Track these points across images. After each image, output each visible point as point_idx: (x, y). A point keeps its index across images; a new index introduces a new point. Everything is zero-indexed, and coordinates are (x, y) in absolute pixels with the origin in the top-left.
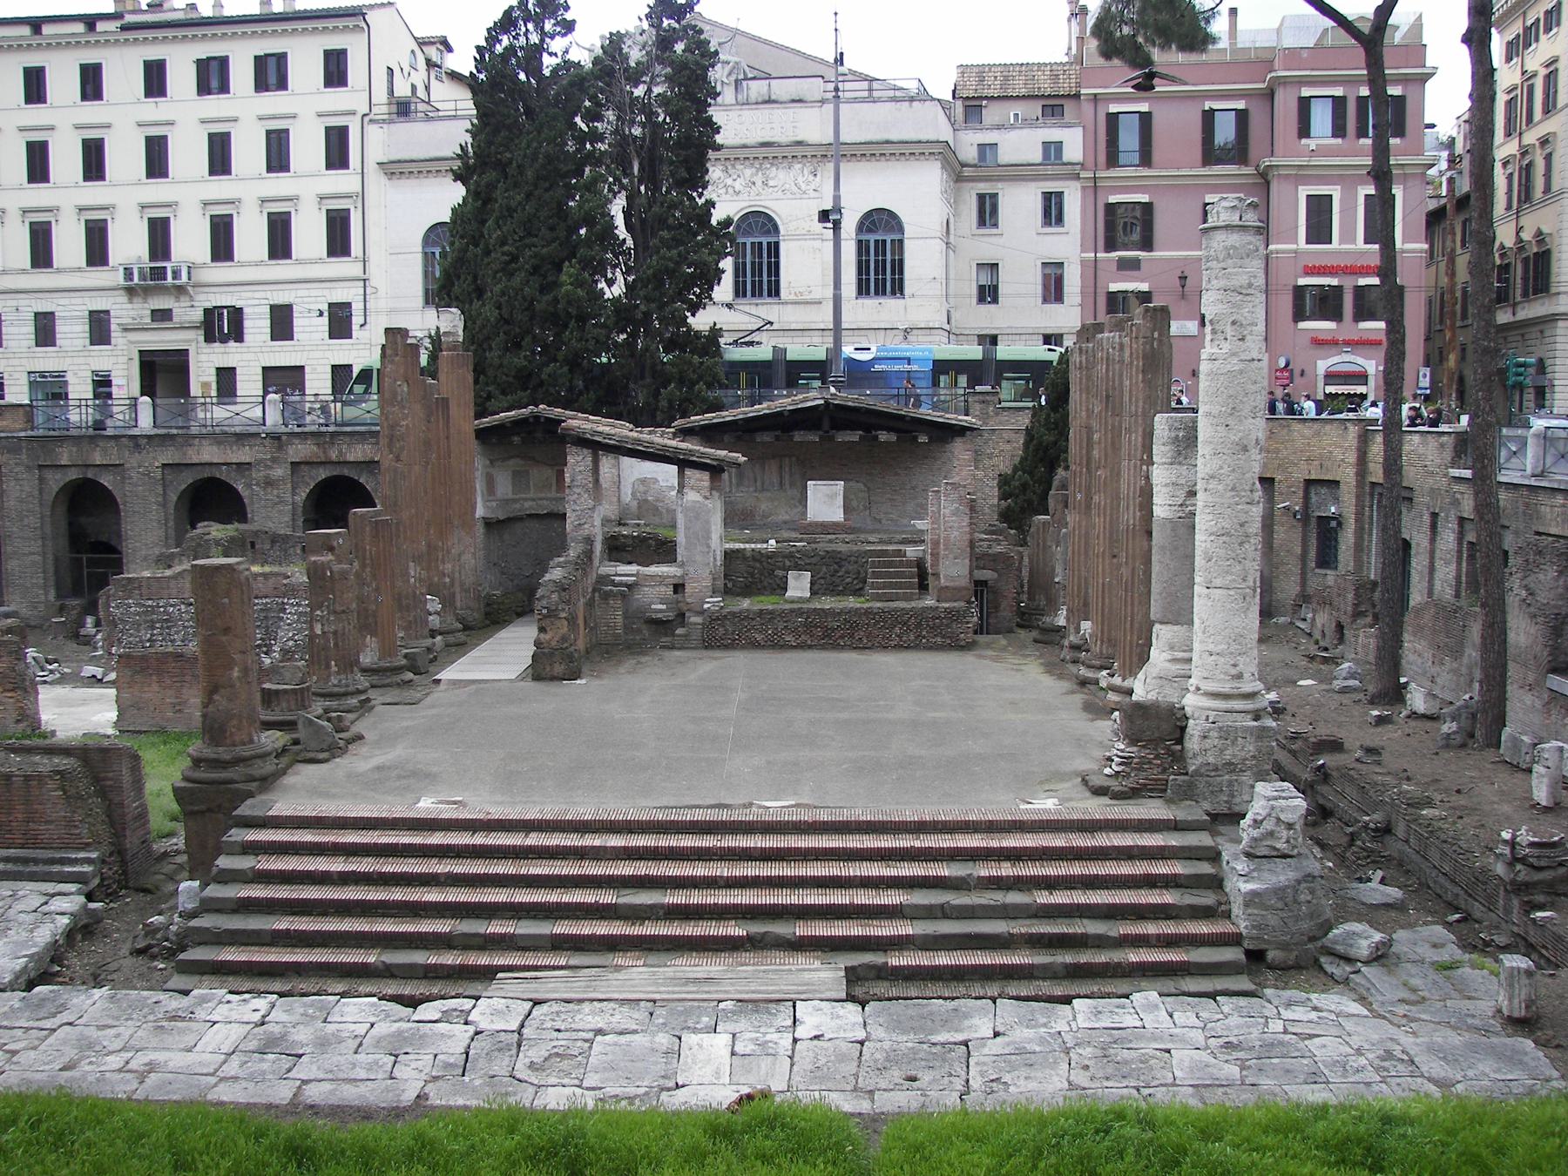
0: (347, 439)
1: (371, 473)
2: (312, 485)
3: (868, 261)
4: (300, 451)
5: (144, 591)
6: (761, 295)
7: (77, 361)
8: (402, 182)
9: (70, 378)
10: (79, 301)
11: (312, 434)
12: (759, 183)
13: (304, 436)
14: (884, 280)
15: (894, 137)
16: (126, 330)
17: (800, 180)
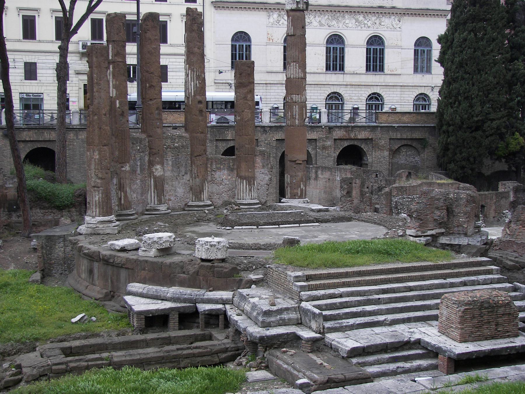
0: (359, 129)
1: (366, 144)
2: (341, 149)
3: (376, 57)
4: (338, 134)
5: (408, 192)
6: (376, 71)
7: (48, 88)
8: (233, 12)
9: (45, 97)
10: (52, 58)
11: (344, 127)
12: (378, 23)
13: (340, 127)
14: (376, 65)
15: (430, 7)
16: (78, 74)
17: (394, 23)
